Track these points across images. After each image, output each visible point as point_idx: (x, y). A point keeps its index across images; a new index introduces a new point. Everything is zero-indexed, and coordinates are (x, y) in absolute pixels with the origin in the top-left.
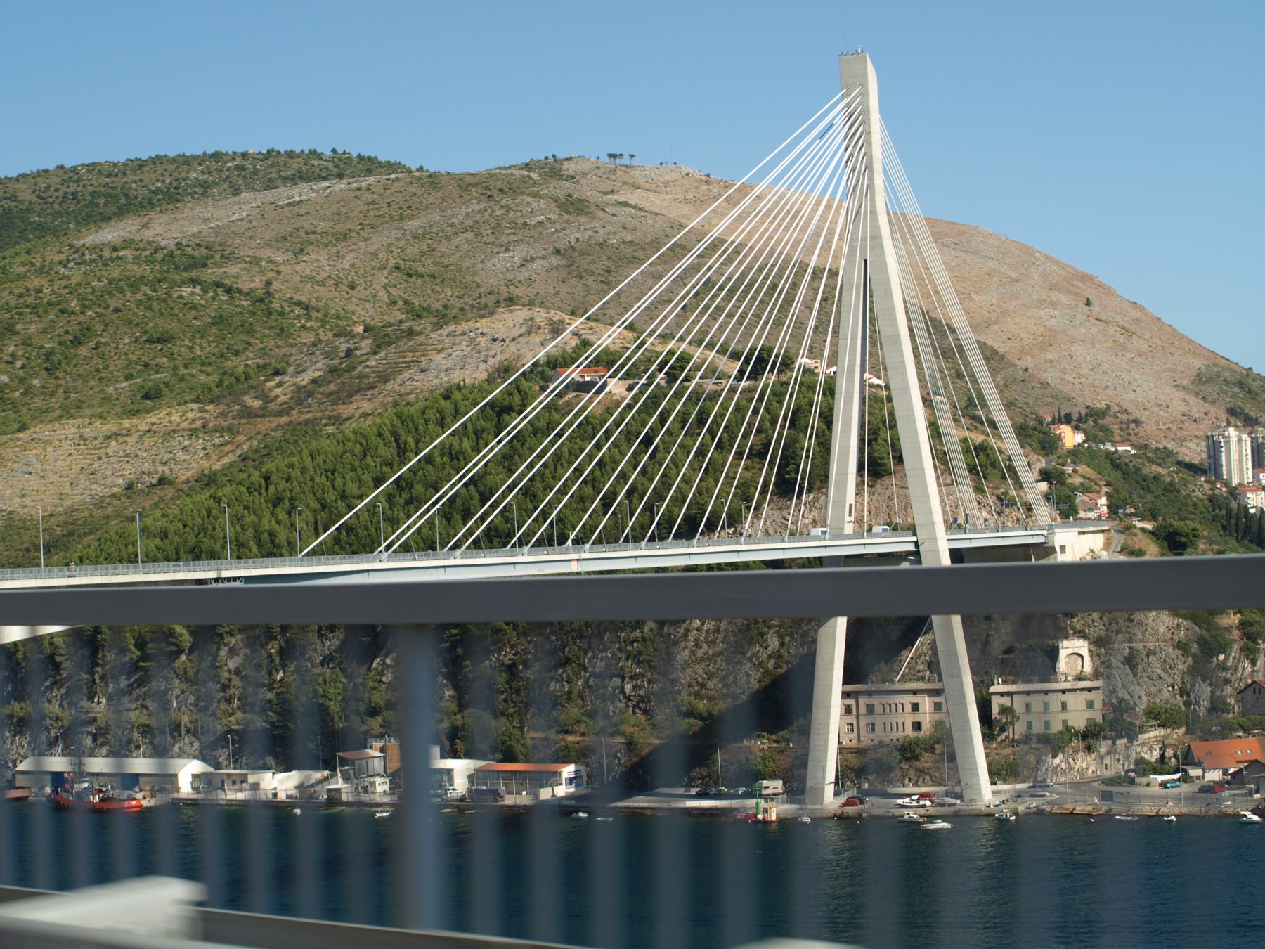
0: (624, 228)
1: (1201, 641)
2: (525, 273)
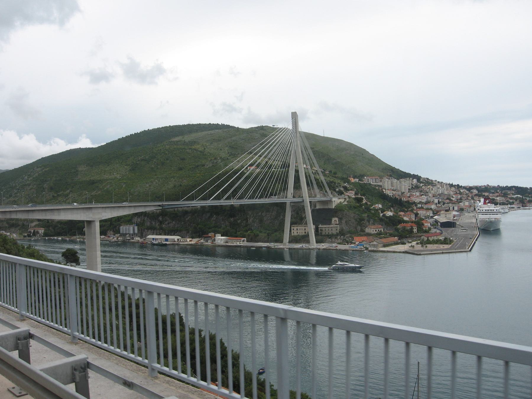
1: (360, 219)
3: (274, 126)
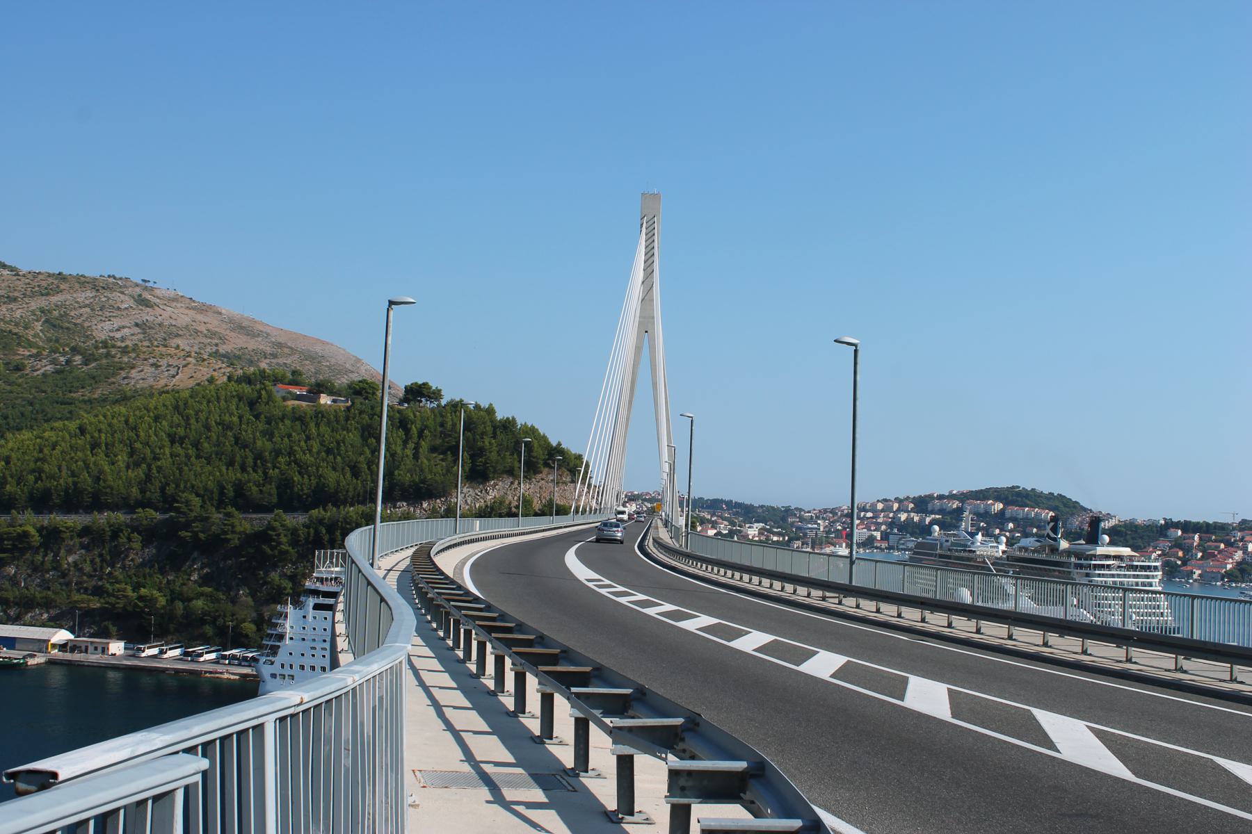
2: (118, 335)
3: (143, 281)
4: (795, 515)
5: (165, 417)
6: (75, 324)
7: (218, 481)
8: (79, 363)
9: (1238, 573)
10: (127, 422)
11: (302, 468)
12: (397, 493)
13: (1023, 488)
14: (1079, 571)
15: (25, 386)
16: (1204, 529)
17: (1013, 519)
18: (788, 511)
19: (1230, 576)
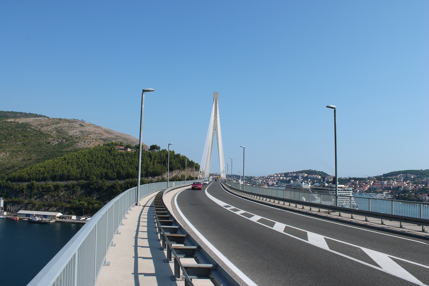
0: (89, 129)
3: (82, 120)
4: (253, 178)
5: (86, 155)
6: (64, 132)
7: (101, 172)
8: (65, 141)
9: (369, 191)
10: (76, 157)
11: (123, 168)
12: (149, 174)
13: (312, 170)
14: (331, 191)
15: (50, 148)
16: (360, 179)
17: (310, 178)
18: (251, 177)
19: (367, 192)
